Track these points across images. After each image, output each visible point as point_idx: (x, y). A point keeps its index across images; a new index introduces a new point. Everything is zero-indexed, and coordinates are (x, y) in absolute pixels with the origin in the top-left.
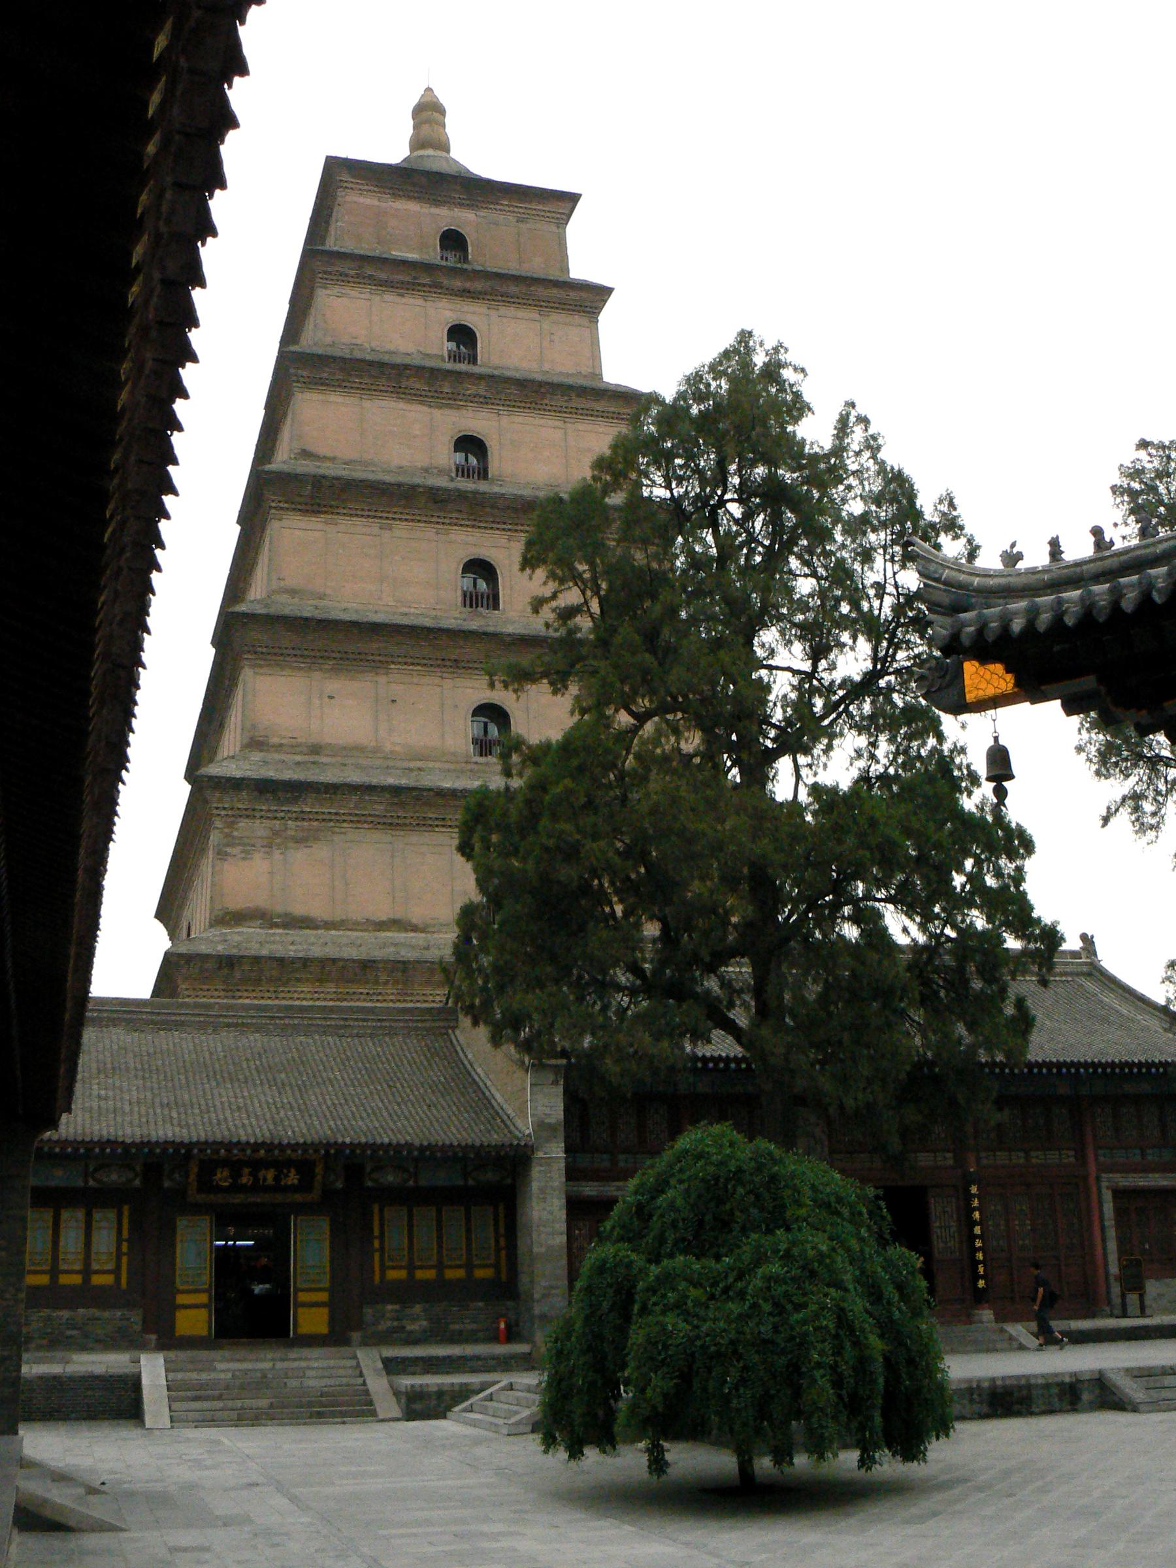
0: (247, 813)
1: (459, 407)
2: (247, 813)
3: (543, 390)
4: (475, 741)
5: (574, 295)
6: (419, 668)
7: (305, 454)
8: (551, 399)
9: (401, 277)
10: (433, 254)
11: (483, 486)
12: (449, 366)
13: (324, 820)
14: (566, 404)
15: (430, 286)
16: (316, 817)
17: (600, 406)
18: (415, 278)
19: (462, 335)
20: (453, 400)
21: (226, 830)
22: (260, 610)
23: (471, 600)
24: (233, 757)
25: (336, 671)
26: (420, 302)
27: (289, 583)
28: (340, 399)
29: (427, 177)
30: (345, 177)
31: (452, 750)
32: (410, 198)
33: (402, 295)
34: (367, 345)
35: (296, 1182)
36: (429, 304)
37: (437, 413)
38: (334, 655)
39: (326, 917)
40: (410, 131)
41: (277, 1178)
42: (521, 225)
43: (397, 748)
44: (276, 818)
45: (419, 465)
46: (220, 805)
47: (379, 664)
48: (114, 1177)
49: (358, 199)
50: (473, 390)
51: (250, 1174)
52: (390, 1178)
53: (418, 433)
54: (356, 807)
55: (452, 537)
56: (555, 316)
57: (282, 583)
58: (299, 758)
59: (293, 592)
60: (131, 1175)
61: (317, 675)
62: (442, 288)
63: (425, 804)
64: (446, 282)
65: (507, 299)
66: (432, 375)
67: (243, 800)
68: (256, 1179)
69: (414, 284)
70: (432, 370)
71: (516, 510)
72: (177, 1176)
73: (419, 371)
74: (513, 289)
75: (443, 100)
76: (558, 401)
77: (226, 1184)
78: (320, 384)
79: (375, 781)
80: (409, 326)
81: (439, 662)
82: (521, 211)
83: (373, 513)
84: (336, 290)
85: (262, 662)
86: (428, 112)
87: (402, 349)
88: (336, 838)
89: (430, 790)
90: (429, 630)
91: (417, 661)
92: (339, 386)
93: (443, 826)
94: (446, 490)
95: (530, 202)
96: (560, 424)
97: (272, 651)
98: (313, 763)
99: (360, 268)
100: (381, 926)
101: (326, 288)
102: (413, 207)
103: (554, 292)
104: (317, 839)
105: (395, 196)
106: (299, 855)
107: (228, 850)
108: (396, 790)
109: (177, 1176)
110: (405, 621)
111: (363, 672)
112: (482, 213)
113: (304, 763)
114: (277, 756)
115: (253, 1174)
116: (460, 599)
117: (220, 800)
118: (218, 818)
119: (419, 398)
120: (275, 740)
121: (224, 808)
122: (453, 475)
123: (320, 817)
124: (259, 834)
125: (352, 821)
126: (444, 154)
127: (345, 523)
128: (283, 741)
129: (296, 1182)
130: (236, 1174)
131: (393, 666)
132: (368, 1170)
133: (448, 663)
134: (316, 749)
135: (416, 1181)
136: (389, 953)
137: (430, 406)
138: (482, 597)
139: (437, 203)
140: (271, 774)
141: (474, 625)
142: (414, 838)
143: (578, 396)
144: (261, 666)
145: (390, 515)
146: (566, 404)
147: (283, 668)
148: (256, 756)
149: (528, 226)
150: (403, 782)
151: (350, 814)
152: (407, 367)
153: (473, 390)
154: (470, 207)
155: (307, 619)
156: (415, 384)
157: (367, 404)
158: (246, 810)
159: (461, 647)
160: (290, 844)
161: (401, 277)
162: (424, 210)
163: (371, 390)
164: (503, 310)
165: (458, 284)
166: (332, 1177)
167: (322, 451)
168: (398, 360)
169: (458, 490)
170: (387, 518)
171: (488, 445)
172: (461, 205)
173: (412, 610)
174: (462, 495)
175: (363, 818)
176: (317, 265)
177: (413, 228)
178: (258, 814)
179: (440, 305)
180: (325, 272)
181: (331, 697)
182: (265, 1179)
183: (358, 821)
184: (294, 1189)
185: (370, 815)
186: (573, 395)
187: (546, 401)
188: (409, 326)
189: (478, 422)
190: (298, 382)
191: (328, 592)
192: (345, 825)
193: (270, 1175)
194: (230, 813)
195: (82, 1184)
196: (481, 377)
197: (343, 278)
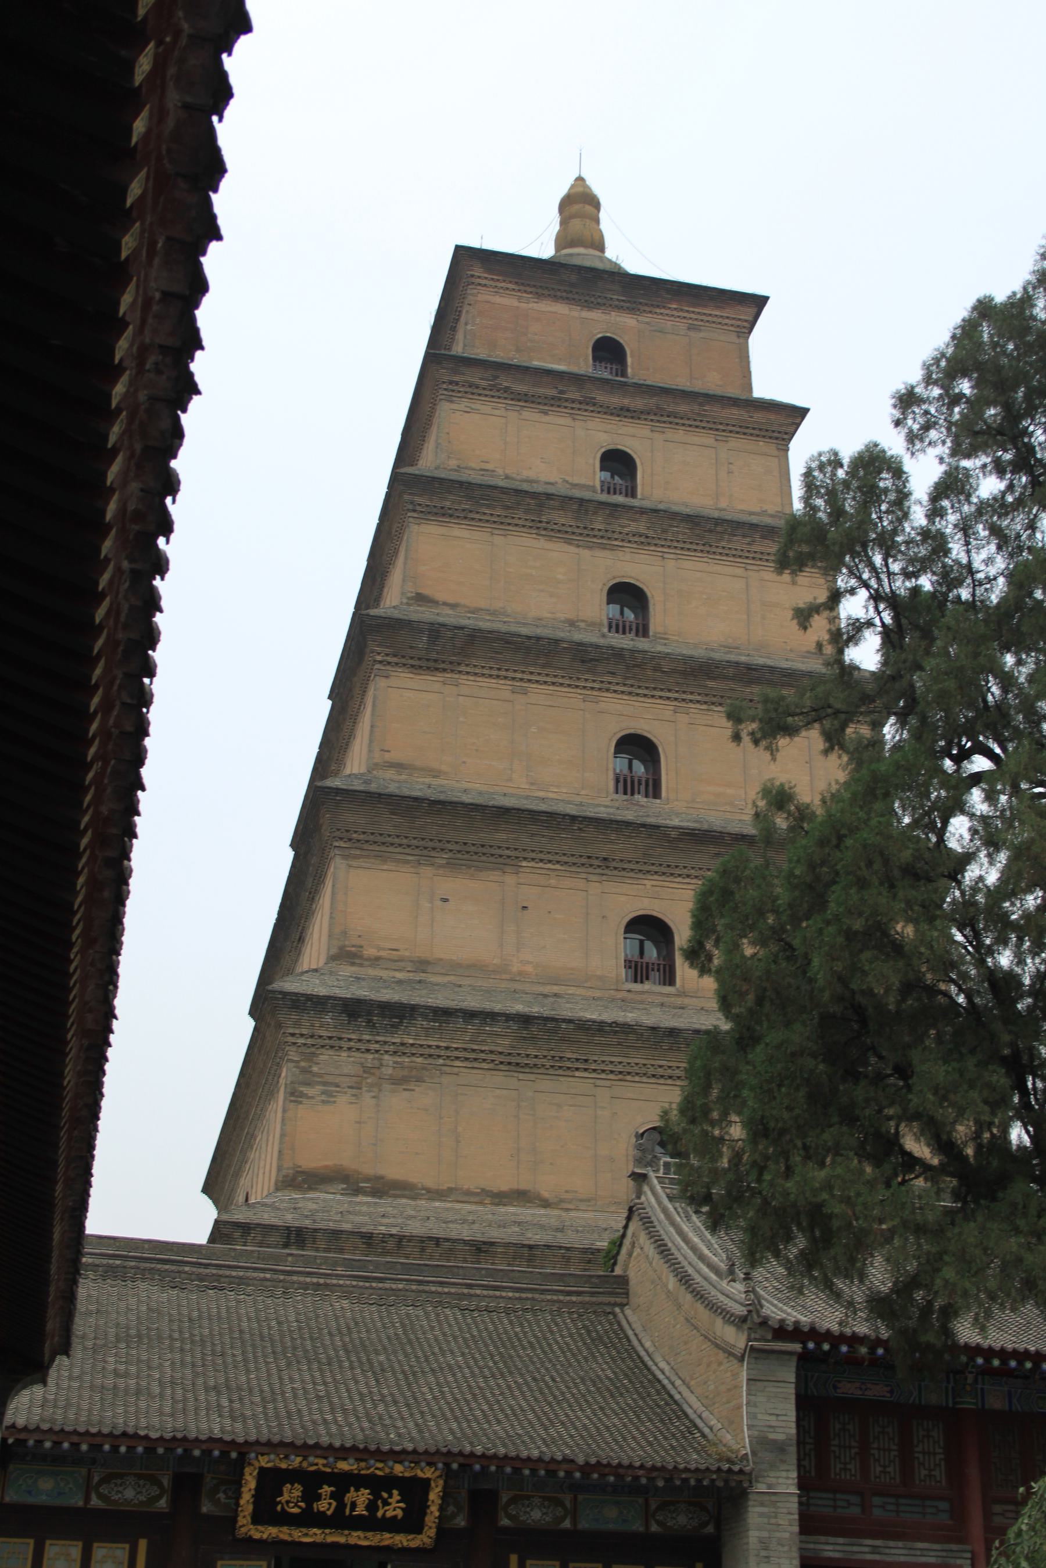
0: (331, 1042)
1: (612, 548)
2: (331, 1042)
3: (719, 529)
4: (628, 963)
5: (759, 416)
6: (557, 867)
7: (421, 599)
8: (729, 541)
9: (542, 391)
10: (584, 364)
11: (642, 644)
12: (604, 497)
13: (430, 1056)
14: (746, 547)
15: (580, 403)
16: (421, 1051)
18: (562, 392)
19: (618, 463)
20: (606, 540)
21: (303, 1064)
22: (358, 786)
23: (625, 785)
24: (316, 970)
25: (451, 866)
26: (568, 421)
27: (394, 756)
28: (465, 534)
29: (577, 273)
30: (478, 271)
31: (598, 973)
32: (556, 298)
33: (546, 413)
34: (500, 471)
35: (399, 1513)
36: (578, 423)
37: (585, 553)
38: (450, 846)
39: (430, 1183)
40: (556, 227)
41: (372, 1507)
42: (692, 334)
43: (529, 968)
44: (368, 1051)
45: (562, 616)
46: (297, 1031)
47: (504, 860)
48: (129, 1493)
49: (491, 300)
50: (633, 527)
51: (333, 1496)
52: (536, 1514)
53: (560, 577)
54: (471, 1041)
55: (602, 705)
56: (735, 443)
57: (387, 756)
58: (400, 975)
59: (399, 766)
60: (155, 1491)
61: (427, 871)
62: (594, 405)
63: (563, 1040)
64: (600, 397)
65: (674, 419)
66: (580, 506)
67: (327, 1024)
68: (341, 1506)
69: (560, 399)
70: (581, 501)
71: (684, 674)
72: (221, 1496)
73: (565, 502)
74: (683, 408)
75: (597, 188)
76: (738, 543)
77: (296, 1510)
79: (498, 1007)
80: (555, 450)
81: (584, 860)
82: (692, 316)
83: (503, 673)
84: (464, 404)
85: (358, 852)
86: (580, 206)
87: (543, 478)
88: (445, 1080)
89: (570, 1021)
90: (574, 818)
91: (557, 858)
93: (586, 1070)
94: (597, 647)
95: (705, 306)
96: (739, 571)
97: (371, 838)
98: (420, 982)
99: (496, 377)
100: (500, 1198)
101: (452, 402)
102: (561, 309)
103: (735, 413)
104: (420, 1080)
105: (539, 296)
106: (396, 1100)
107: (304, 1089)
108: (525, 1020)
109: (221, 1496)
110: (543, 807)
111: (487, 869)
112: (646, 318)
113: (410, 981)
114: (372, 972)
115: (338, 1496)
116: (611, 784)
117: (297, 1024)
118: (294, 1049)
120: (370, 952)
121: (302, 1035)
122: (606, 630)
123: (427, 1051)
124: (346, 1071)
125: (467, 1059)
126: (599, 254)
127: (468, 684)
128: (383, 954)
129: (399, 1513)
130: (310, 1496)
131: (524, 864)
132: (504, 1498)
133: (596, 862)
134: (422, 965)
135: (574, 1522)
136: (510, 1234)
137: (578, 546)
138: (640, 784)
139: (589, 305)
140: (362, 992)
141: (629, 815)
142: (546, 1084)
143: (763, 537)
144: (356, 857)
145: (526, 677)
146: (746, 547)
147: (385, 861)
148: (347, 970)
149: (702, 335)
150: (535, 1010)
151: (465, 1049)
152: (549, 496)
153: (633, 527)
154: (633, 310)
155: (416, 799)
156: (561, 518)
157: (498, 540)
158: (330, 1038)
159: (611, 842)
160: (387, 1086)
161: (542, 391)
162: (575, 314)
163: (501, 524)
164: (670, 434)
165: (615, 400)
166: (451, 1509)
167: (441, 597)
168: (539, 488)
169: (612, 648)
170: (521, 680)
171: (649, 594)
172: (619, 308)
173: (551, 795)
174: (617, 654)
175: (483, 1056)
176: (444, 374)
177: (559, 334)
178: (345, 1045)
179: (590, 425)
180: (451, 383)
181: (446, 900)
182: (354, 1505)
183: (474, 1058)
184: (391, 1525)
185: (491, 1052)
186: (757, 536)
187: (723, 544)
188: (555, 450)
190: (414, 511)
191: (444, 768)
192: (457, 1063)
193: (360, 1498)
194: (310, 1041)
195: (81, 1503)
196: (642, 511)
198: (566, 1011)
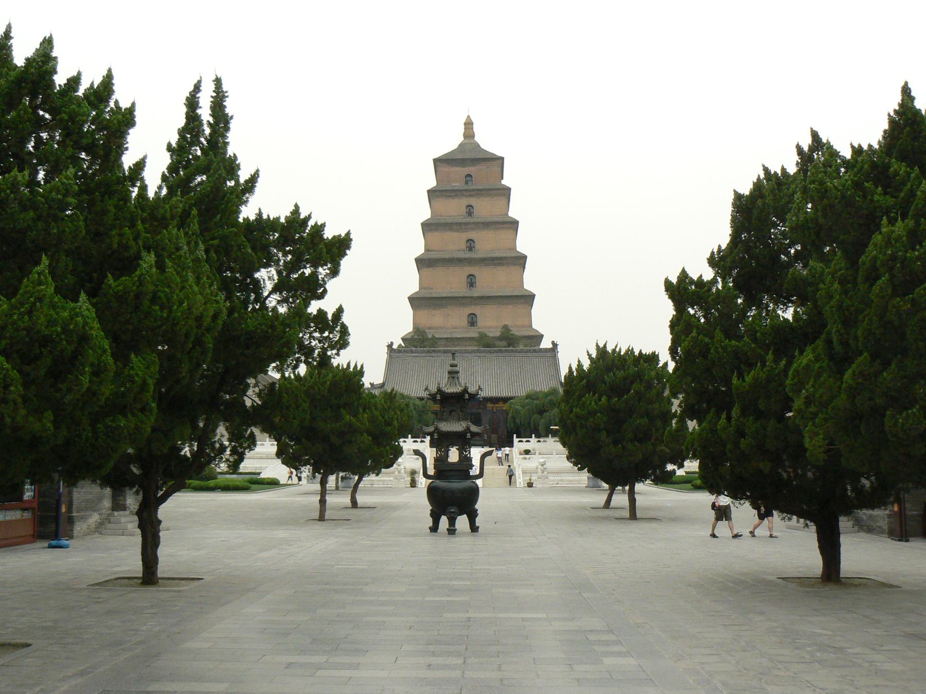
17: (506, 226)
49: (445, 169)
59: (425, 288)
65: (482, 195)
66: (460, 224)
78: (430, 230)
86: (469, 125)
92: (436, 230)
102: (457, 169)
108: (447, 339)
119: (457, 231)
141: (467, 295)
165: (468, 194)
189: (472, 235)
197: (438, 196)
198: (454, 336)
